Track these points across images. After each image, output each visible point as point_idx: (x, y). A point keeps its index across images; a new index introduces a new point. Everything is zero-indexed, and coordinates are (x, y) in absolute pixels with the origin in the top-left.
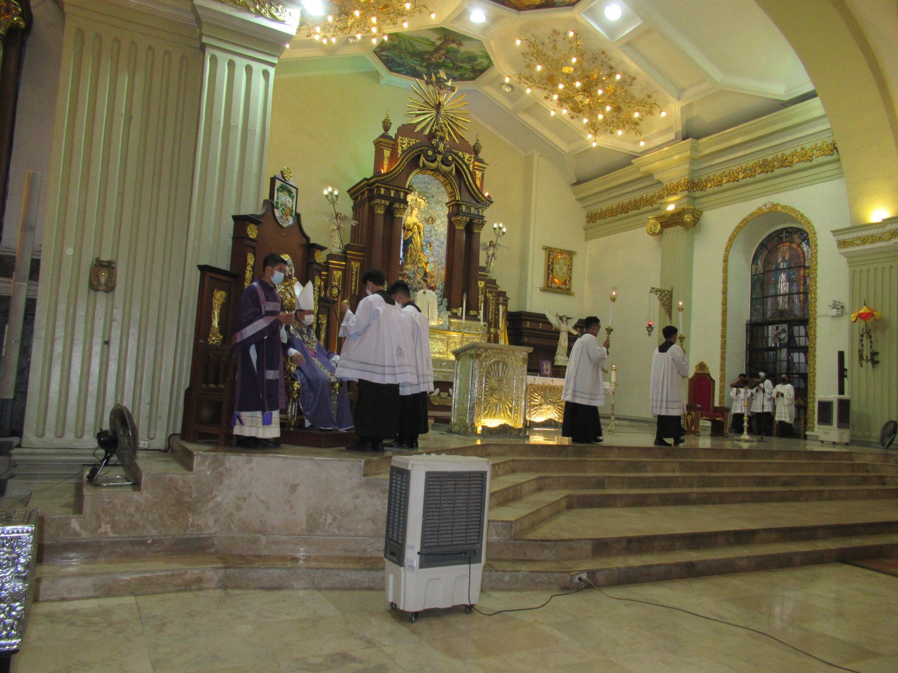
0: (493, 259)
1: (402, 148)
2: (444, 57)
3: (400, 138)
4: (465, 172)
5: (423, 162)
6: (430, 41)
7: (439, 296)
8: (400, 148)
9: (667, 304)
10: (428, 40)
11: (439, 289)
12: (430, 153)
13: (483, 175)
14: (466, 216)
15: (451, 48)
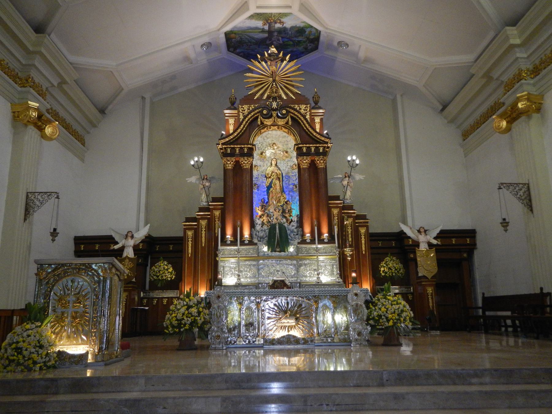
0: (349, 187)
1: (243, 113)
2: (280, 38)
3: (240, 106)
4: (300, 119)
5: (261, 121)
6: (259, 29)
7: (295, 227)
8: (241, 114)
9: (523, 198)
10: (257, 28)
11: (295, 221)
12: (265, 112)
13: (321, 119)
14: (306, 156)
15: (278, 28)
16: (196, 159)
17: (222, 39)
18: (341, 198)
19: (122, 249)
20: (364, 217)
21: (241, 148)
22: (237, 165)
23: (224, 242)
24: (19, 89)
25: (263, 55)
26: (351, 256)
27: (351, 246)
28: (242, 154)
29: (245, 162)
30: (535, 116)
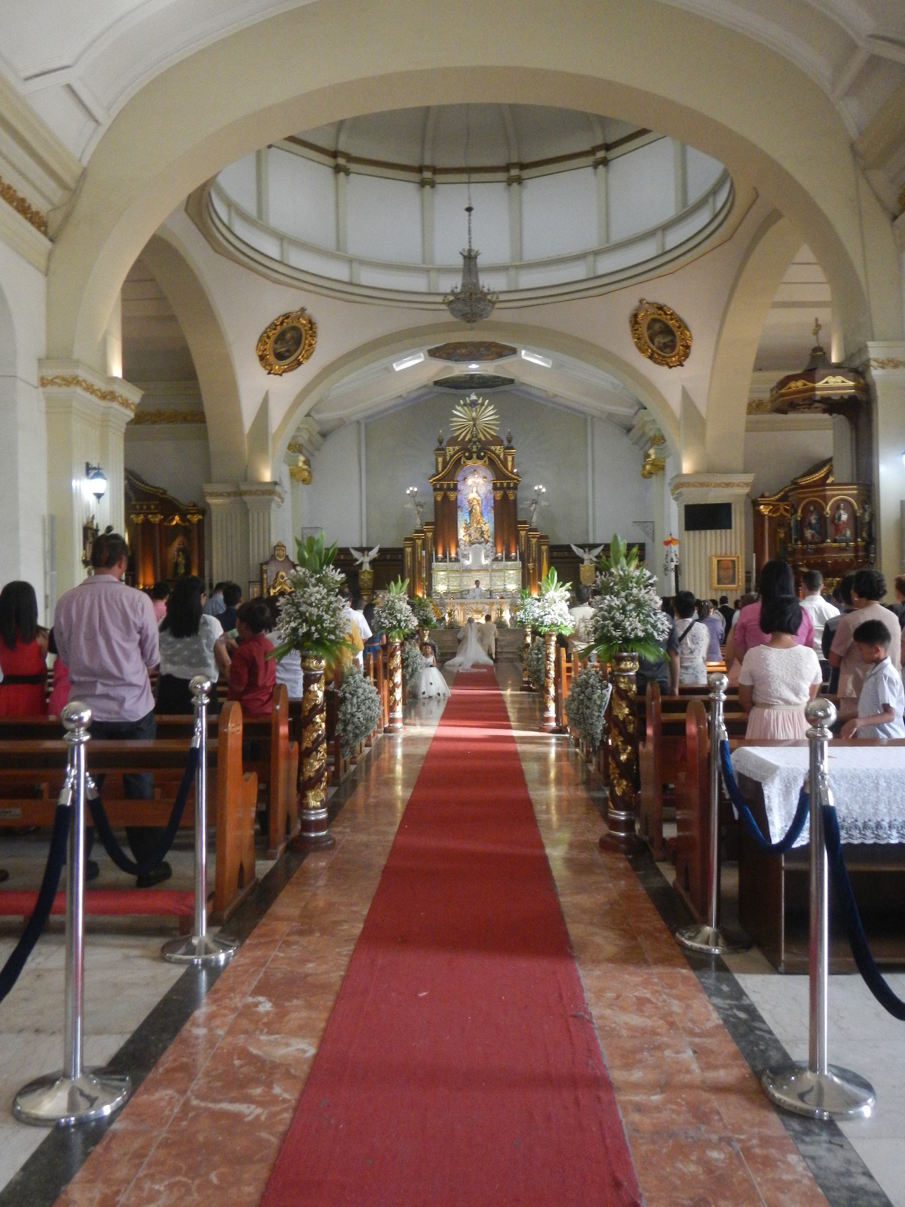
12: (467, 454)
13: (513, 458)
16: (411, 489)
17: (431, 383)
18: (528, 522)
19: (361, 564)
20: (546, 537)
21: (448, 484)
22: (445, 497)
23: (437, 560)
24: (293, 454)
25: (465, 400)
26: (533, 569)
27: (534, 561)
28: (449, 489)
29: (452, 495)
30: (660, 472)
